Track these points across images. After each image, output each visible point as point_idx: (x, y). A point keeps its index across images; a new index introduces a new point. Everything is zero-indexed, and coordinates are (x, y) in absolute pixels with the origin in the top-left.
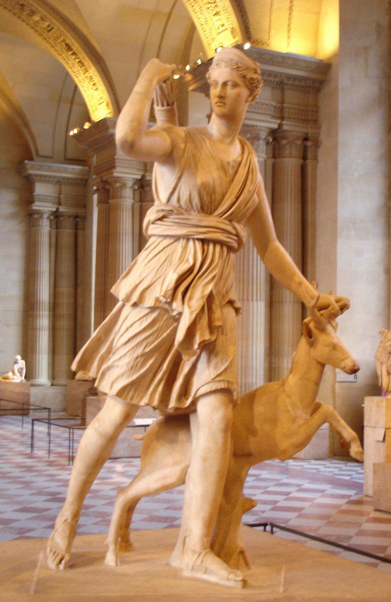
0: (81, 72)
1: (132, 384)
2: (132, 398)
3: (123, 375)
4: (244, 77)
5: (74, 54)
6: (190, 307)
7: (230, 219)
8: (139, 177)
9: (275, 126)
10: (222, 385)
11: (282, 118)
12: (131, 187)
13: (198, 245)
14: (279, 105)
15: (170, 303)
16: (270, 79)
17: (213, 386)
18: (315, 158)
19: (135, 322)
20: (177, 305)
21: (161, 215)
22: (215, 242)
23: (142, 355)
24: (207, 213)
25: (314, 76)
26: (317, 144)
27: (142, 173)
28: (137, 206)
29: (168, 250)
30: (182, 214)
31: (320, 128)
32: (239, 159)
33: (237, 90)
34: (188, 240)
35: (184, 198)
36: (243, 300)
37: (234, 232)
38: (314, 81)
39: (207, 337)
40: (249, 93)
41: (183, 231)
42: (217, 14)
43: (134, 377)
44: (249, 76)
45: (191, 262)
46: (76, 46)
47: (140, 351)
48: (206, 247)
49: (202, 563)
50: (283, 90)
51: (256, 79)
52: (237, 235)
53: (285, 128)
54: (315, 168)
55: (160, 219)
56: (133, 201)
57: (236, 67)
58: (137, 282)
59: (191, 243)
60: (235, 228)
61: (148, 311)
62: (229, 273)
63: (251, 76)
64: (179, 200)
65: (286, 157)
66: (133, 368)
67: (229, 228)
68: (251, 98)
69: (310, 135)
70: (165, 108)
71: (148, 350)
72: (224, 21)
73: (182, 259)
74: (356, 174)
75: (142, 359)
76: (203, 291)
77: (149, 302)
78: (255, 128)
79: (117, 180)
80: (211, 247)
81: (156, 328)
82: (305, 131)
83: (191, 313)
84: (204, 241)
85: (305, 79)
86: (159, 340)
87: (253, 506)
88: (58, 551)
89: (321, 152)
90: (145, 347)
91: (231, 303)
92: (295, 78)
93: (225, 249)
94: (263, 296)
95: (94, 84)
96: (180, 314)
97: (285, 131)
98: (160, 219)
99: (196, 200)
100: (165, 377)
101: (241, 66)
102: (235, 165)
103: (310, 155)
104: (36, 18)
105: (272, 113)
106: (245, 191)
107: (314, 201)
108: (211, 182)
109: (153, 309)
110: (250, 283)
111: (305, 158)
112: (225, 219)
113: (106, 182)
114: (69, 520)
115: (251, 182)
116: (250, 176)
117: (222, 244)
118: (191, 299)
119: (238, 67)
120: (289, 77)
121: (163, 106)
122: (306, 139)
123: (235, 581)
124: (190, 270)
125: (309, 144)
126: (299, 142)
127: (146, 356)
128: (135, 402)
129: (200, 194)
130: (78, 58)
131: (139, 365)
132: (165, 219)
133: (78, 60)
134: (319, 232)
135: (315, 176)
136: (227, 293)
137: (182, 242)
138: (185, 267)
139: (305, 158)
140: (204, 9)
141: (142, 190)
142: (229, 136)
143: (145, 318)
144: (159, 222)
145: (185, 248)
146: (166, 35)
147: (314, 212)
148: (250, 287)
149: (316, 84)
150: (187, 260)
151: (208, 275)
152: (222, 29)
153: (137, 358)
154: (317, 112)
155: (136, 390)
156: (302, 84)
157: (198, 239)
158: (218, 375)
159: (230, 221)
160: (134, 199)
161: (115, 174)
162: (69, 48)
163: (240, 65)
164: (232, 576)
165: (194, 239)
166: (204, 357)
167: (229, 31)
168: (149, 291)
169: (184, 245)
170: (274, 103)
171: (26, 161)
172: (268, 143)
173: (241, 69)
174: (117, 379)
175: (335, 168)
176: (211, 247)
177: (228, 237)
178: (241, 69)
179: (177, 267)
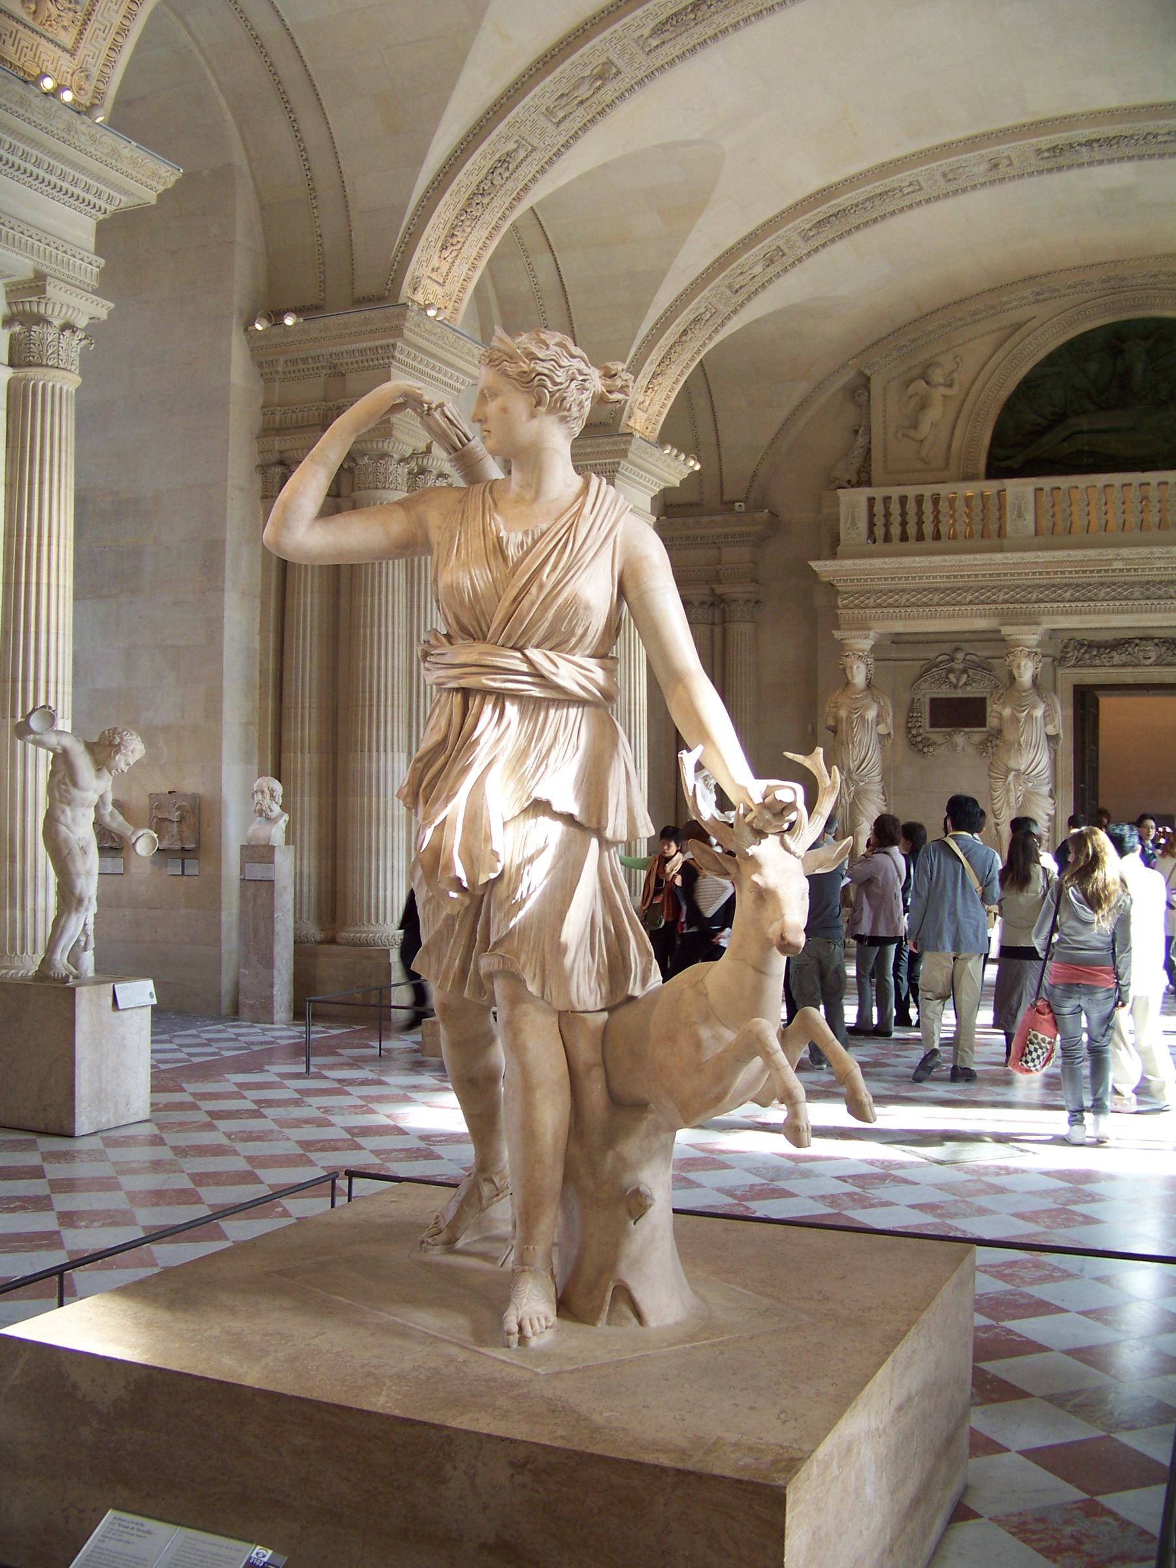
4: (505, 374)
13: (458, 699)
24: (479, 639)
30: (443, 645)
37: (524, 668)
40: (534, 402)
51: (531, 372)
57: (488, 360)
63: (520, 370)
68: (542, 409)
84: (466, 693)
101: (500, 354)
119: (490, 361)
142: (529, 485)
157: (457, 690)
159: (520, 650)
173: (497, 362)
178: (497, 362)
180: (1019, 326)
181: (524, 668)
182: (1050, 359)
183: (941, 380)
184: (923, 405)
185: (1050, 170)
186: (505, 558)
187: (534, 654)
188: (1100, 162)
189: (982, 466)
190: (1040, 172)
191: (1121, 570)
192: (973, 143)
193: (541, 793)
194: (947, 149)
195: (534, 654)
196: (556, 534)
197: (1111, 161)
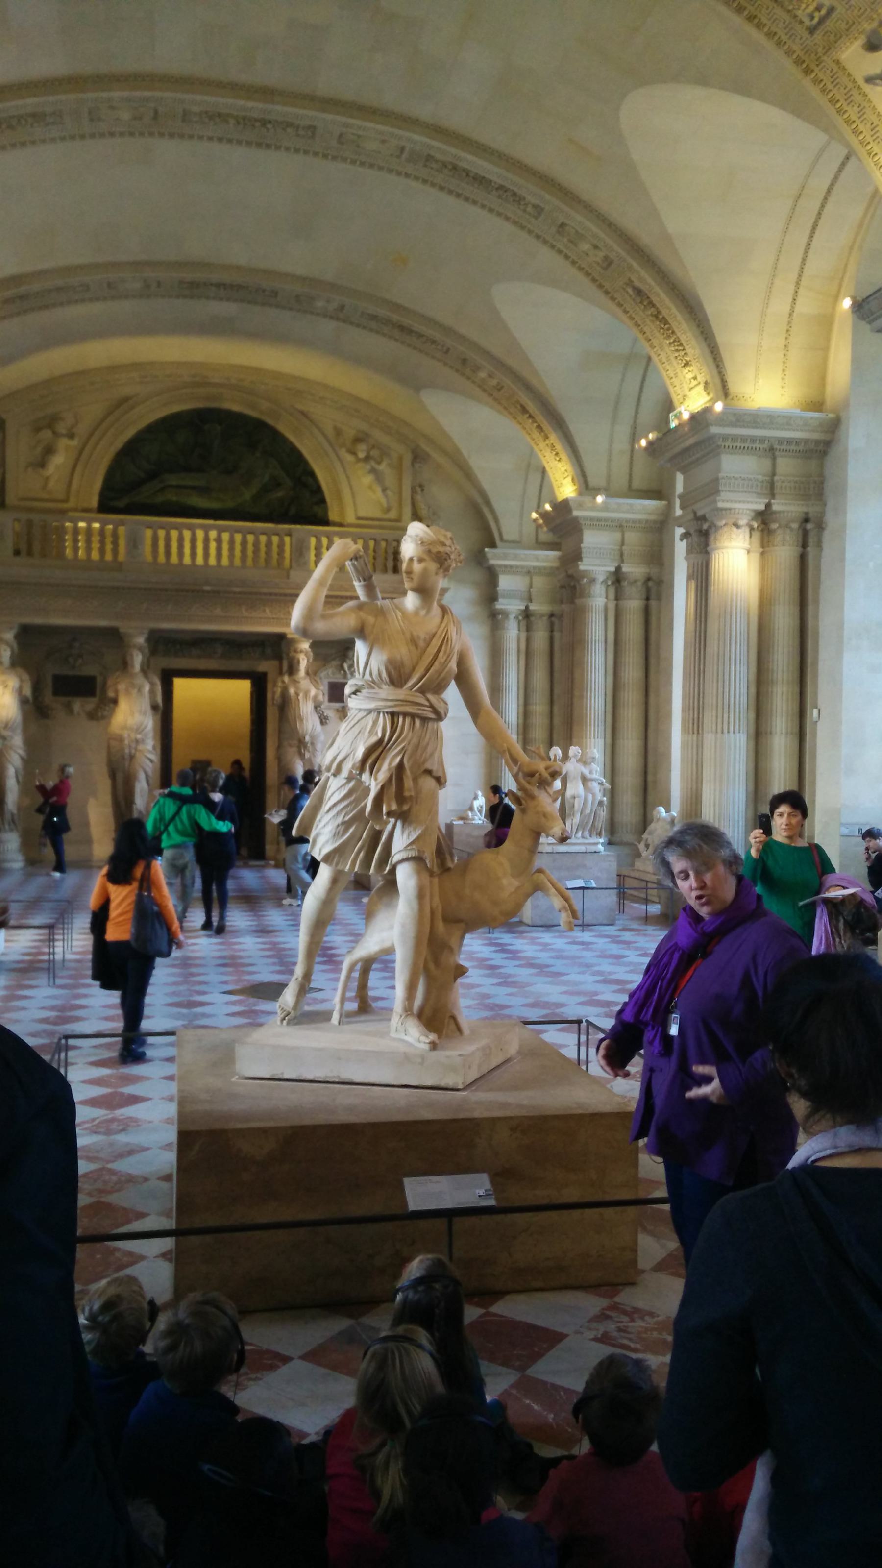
0: (541, 439)
1: (335, 851)
2: (337, 865)
3: (327, 842)
5: (531, 417)
6: (376, 779)
7: (423, 691)
8: (613, 569)
9: (762, 507)
10: (412, 854)
11: (773, 495)
12: (602, 582)
14: (768, 478)
15: (360, 774)
16: (754, 446)
17: (404, 855)
18: (819, 545)
19: (334, 792)
20: (365, 777)
21: (353, 689)
22: (405, 715)
23: (343, 823)
25: (816, 436)
26: (821, 527)
27: (617, 565)
28: (612, 605)
29: (363, 722)
30: (374, 688)
31: (825, 505)
32: (434, 631)
33: (423, 565)
34: (379, 713)
35: (375, 673)
36: (717, 732)
37: (427, 704)
38: (817, 442)
39: (394, 807)
41: (372, 705)
42: (687, 364)
43: (337, 844)
44: (434, 550)
45: (380, 735)
46: (532, 407)
47: (340, 820)
48: (396, 720)
49: (402, 1024)
50: (774, 459)
52: (431, 706)
53: (775, 507)
54: (818, 558)
55: (355, 693)
56: (606, 600)
58: (335, 754)
59: (381, 715)
60: (428, 700)
61: (345, 781)
62: (428, 744)
64: (371, 674)
65: (777, 546)
66: (336, 835)
67: (421, 700)
69: (811, 515)
70: (362, 583)
71: (347, 818)
72: (696, 372)
73: (372, 732)
74: (871, 564)
75: (343, 827)
76: (390, 764)
77: (345, 773)
78: (733, 511)
79: (584, 574)
80: (401, 719)
81: (353, 798)
82: (805, 509)
83: (377, 785)
84: (393, 715)
85: (806, 441)
86: (357, 809)
87: (465, 973)
88: (285, 1008)
89: (827, 536)
90: (344, 817)
91: (429, 772)
92: (789, 441)
93: (418, 722)
94: (744, 727)
95: (557, 454)
96: (370, 785)
97: (775, 512)
98: (355, 693)
99: (384, 675)
100: (367, 845)
102: (427, 637)
103: (812, 540)
104: (483, 375)
105: (759, 490)
106: (436, 663)
107: (817, 602)
108: (398, 657)
109: (349, 779)
110: (726, 709)
111: (804, 545)
112: (416, 691)
113: (570, 577)
114: (300, 979)
115: (445, 652)
116: (443, 648)
117: (413, 716)
118: (379, 770)
120: (781, 441)
121: (360, 581)
122: (806, 520)
123: (425, 1043)
124: (380, 742)
125: (809, 526)
126: (795, 526)
127: (347, 825)
128: (340, 867)
129: (387, 669)
130: (536, 422)
131: (341, 832)
132: (358, 693)
133: (535, 425)
134: (822, 643)
135: (818, 568)
136: (424, 763)
137: (373, 716)
138: (374, 739)
139: (804, 545)
140: (672, 358)
141: (617, 584)
143: (343, 788)
144: (353, 696)
145: (375, 723)
146: (647, 383)
147: (816, 617)
148: (726, 716)
149: (821, 447)
150: (377, 733)
151: (395, 748)
152: (694, 383)
153: (338, 826)
154: (822, 483)
155: (340, 857)
156: (801, 448)
157: (387, 713)
158: (411, 844)
160: (607, 598)
161: (582, 568)
162: (524, 410)
163: (425, 540)
164: (423, 1039)
165: (383, 713)
166: (399, 824)
167: (701, 386)
168: (345, 762)
169: (374, 718)
170: (760, 477)
171: (486, 549)
172: (752, 529)
174: (323, 846)
175: (842, 559)
176: (401, 719)
177: (420, 709)
179: (367, 739)
180: (126, 399)
181: (427, 704)
182: (152, 430)
183: (64, 431)
184: (49, 451)
185: (185, 297)
186: (416, 646)
187: (430, 696)
188: (221, 299)
189: (94, 502)
190: (178, 297)
191: (208, 592)
192: (137, 265)
193: (428, 766)
194: (116, 265)
195: (430, 696)
196: (440, 636)
197: (228, 300)
